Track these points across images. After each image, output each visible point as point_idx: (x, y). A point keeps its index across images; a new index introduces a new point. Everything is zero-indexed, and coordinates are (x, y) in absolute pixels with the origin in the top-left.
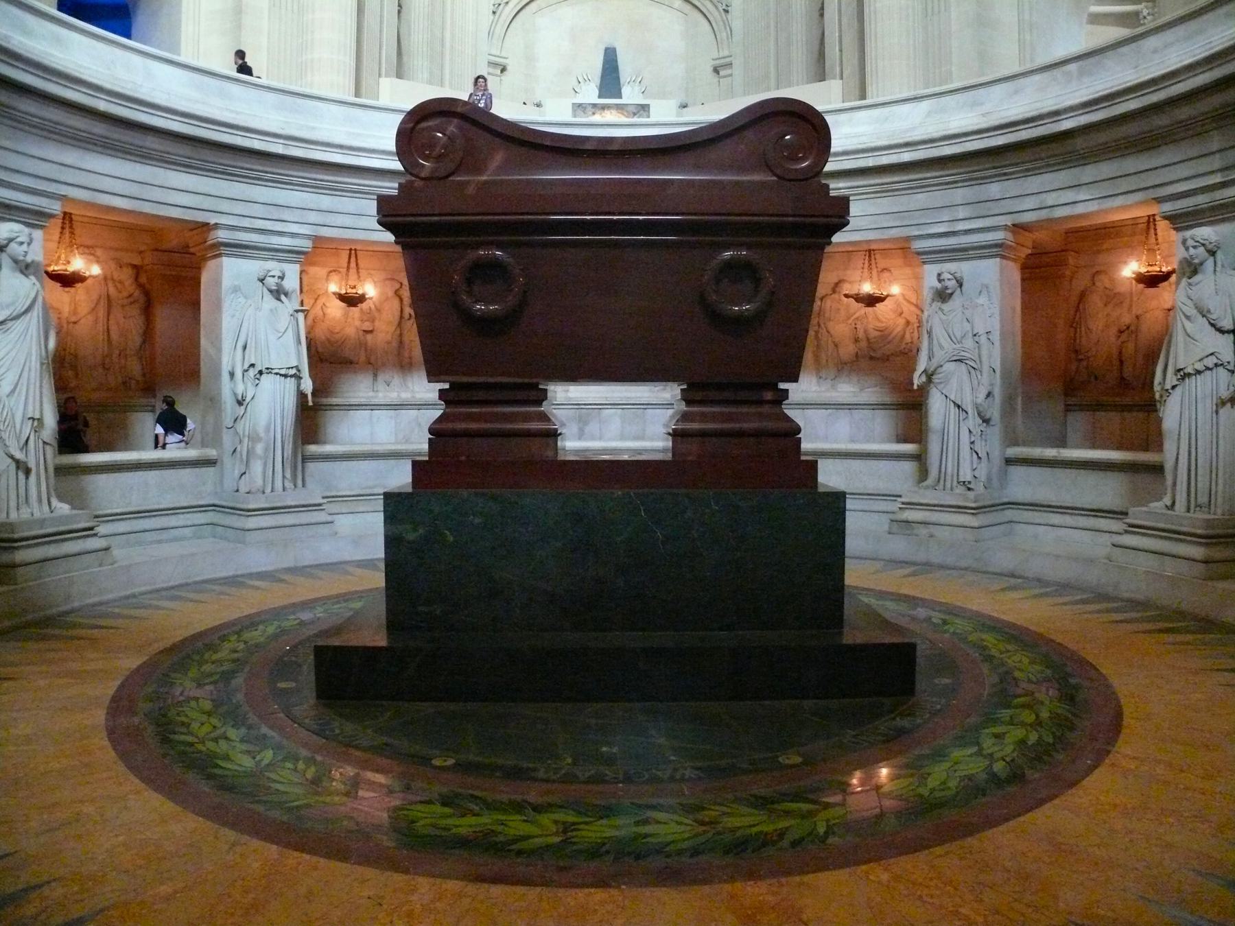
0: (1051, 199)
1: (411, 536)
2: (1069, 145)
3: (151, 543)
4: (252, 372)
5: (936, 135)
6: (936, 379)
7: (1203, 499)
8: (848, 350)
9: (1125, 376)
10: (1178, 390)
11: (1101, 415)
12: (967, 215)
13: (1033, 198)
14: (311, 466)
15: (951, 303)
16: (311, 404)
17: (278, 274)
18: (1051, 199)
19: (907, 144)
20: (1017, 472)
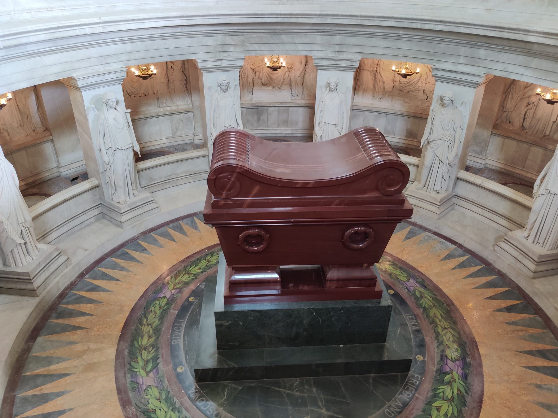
0: (511, 68)
1: (226, 324)
2: (528, 46)
3: (78, 231)
4: (110, 151)
5: (458, 21)
6: (432, 145)
7: (541, 241)
8: (389, 86)
9: (524, 125)
10: (544, 197)
11: (508, 141)
12: (464, 62)
13: (501, 65)
14: (142, 173)
15: (446, 109)
16: (140, 156)
17: (118, 108)
18: (511, 68)
19: (441, 21)
20: (461, 184)
